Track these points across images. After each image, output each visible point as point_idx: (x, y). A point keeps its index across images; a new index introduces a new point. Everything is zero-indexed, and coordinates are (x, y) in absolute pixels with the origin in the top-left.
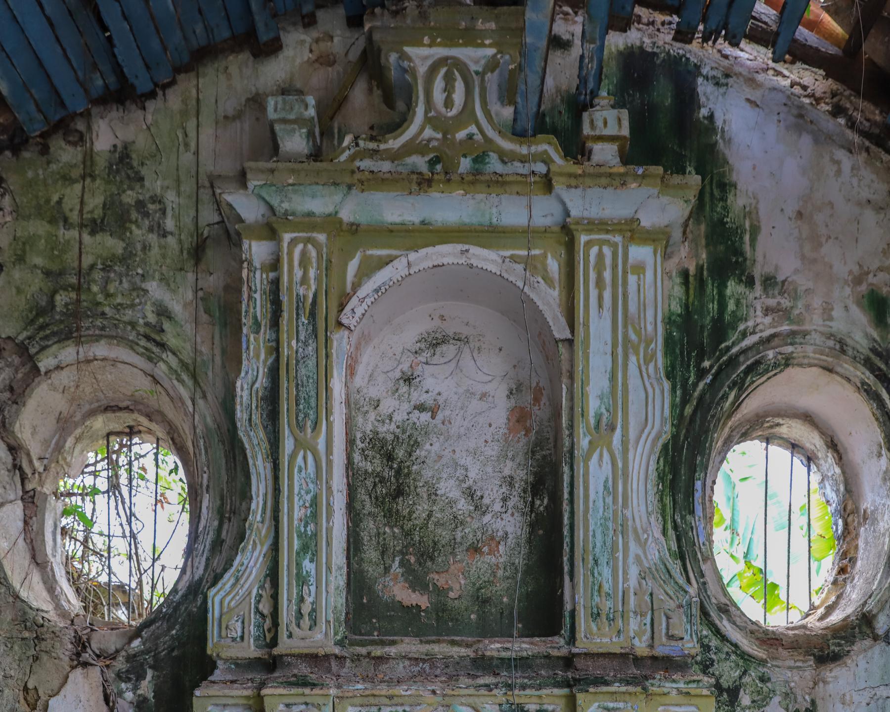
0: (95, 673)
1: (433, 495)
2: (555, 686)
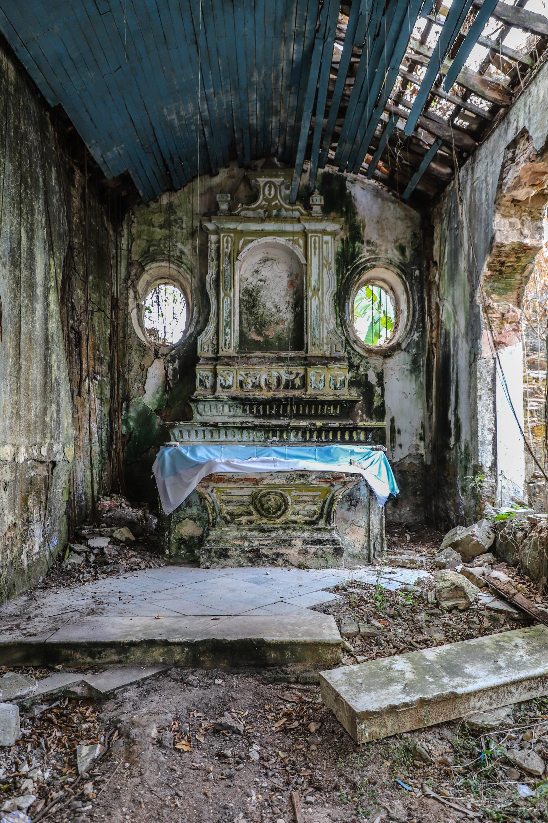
0: (162, 360)
1: (264, 307)
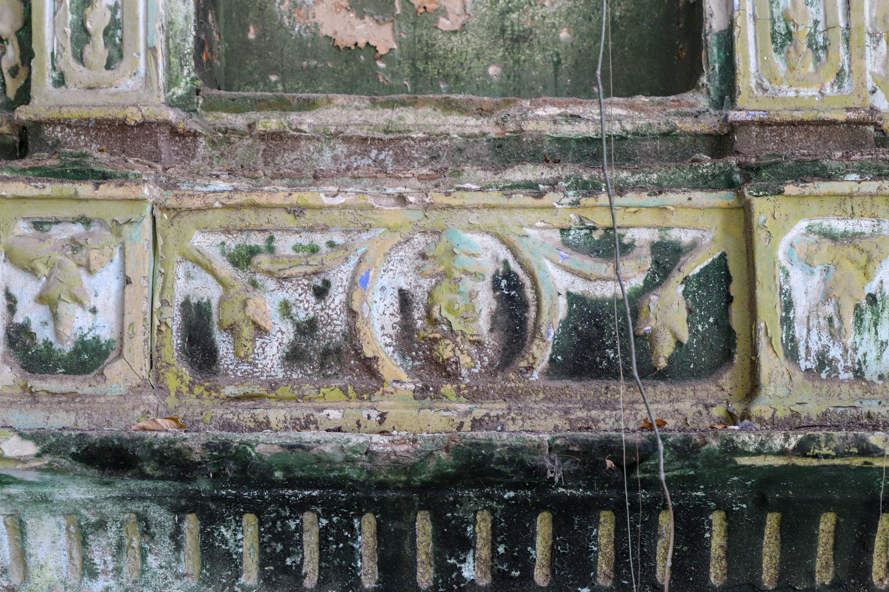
2: (695, 188)
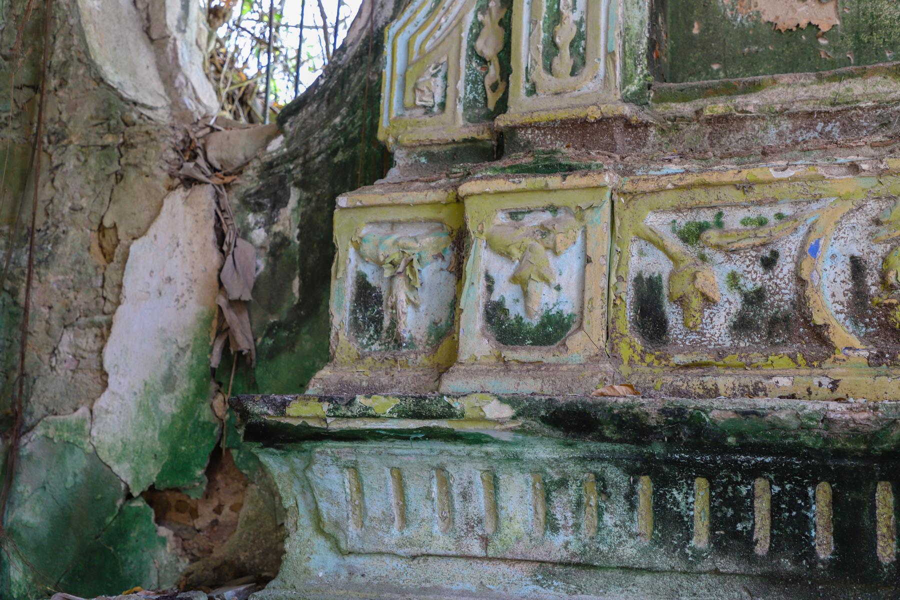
0: (204, 196)
